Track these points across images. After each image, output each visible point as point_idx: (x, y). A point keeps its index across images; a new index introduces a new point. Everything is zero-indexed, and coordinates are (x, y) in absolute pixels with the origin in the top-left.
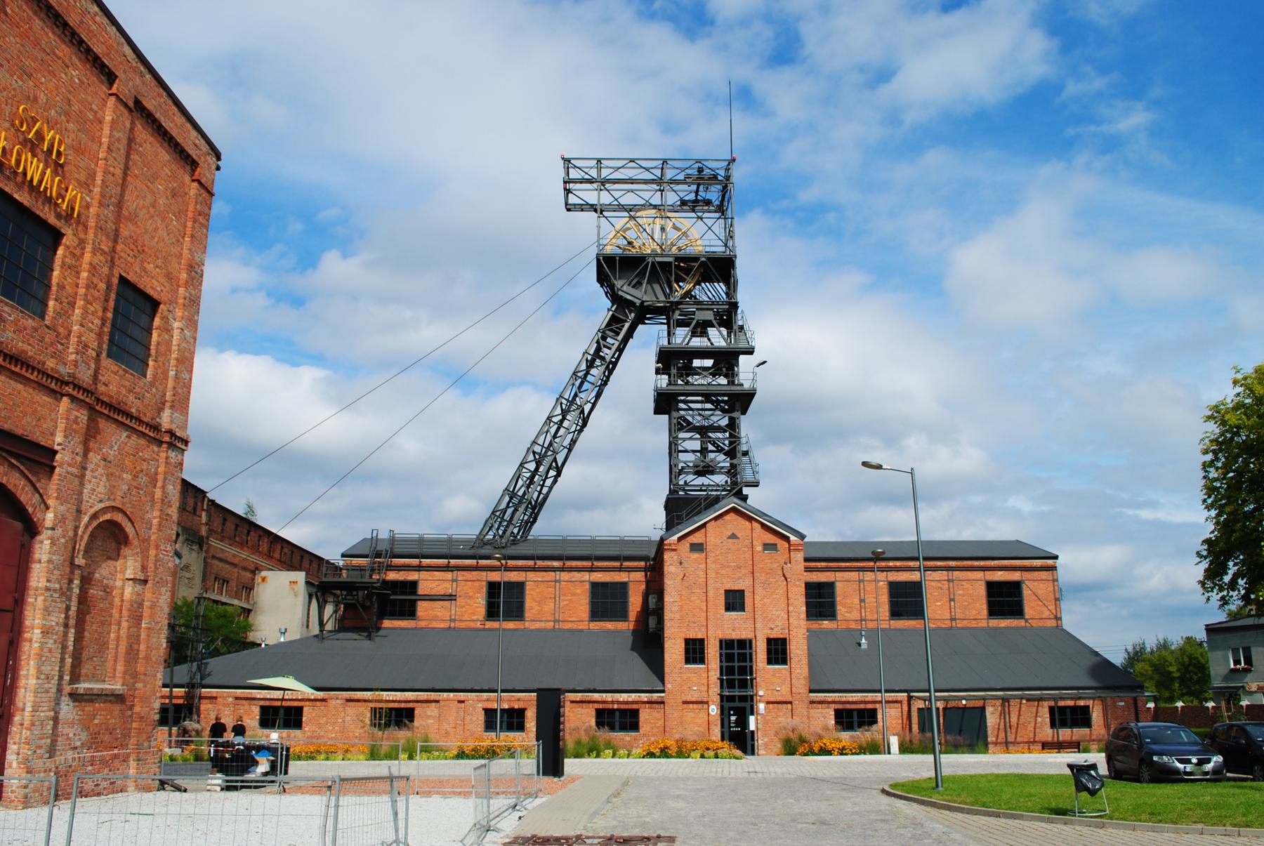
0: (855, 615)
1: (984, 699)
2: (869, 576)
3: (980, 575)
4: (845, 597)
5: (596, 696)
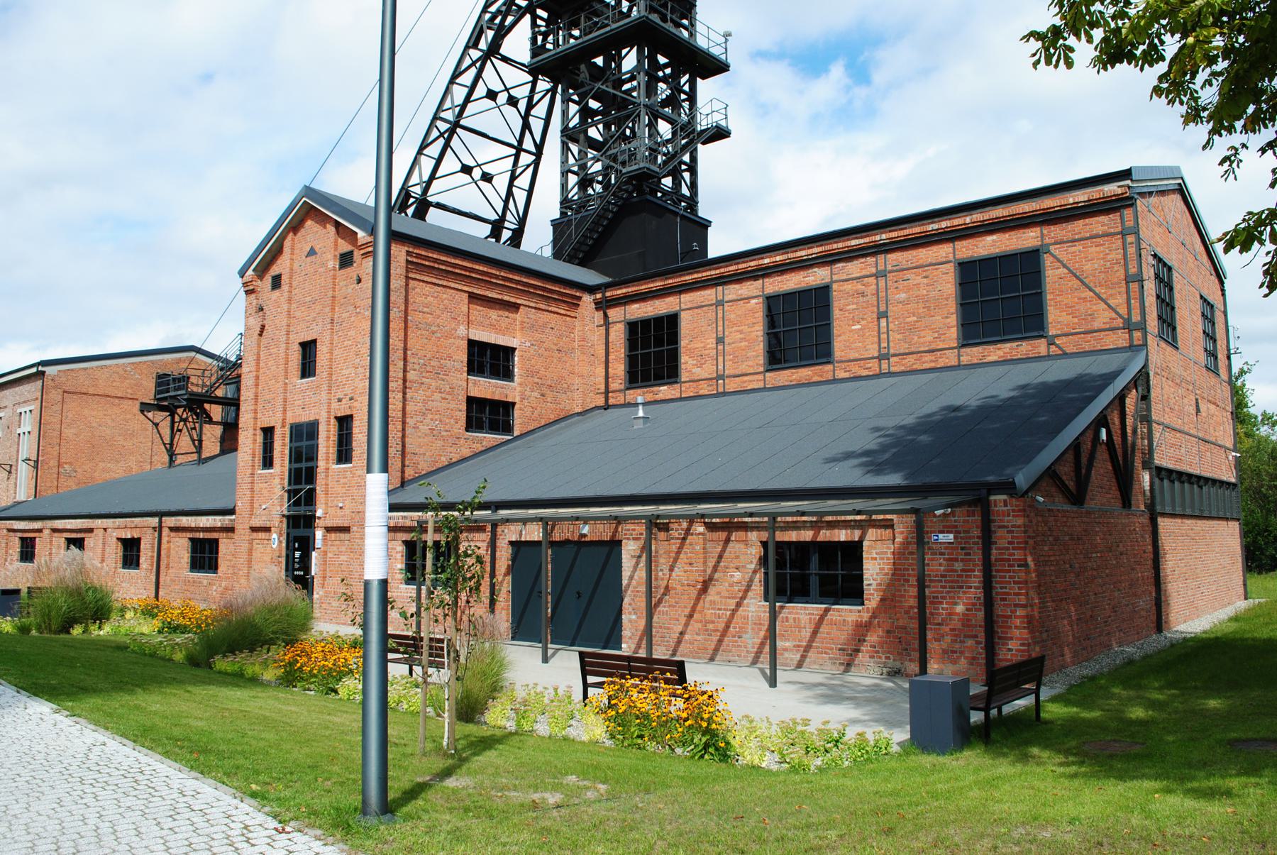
0: (708, 370)
1: (618, 520)
2: (733, 291)
4: (694, 338)
5: (185, 521)
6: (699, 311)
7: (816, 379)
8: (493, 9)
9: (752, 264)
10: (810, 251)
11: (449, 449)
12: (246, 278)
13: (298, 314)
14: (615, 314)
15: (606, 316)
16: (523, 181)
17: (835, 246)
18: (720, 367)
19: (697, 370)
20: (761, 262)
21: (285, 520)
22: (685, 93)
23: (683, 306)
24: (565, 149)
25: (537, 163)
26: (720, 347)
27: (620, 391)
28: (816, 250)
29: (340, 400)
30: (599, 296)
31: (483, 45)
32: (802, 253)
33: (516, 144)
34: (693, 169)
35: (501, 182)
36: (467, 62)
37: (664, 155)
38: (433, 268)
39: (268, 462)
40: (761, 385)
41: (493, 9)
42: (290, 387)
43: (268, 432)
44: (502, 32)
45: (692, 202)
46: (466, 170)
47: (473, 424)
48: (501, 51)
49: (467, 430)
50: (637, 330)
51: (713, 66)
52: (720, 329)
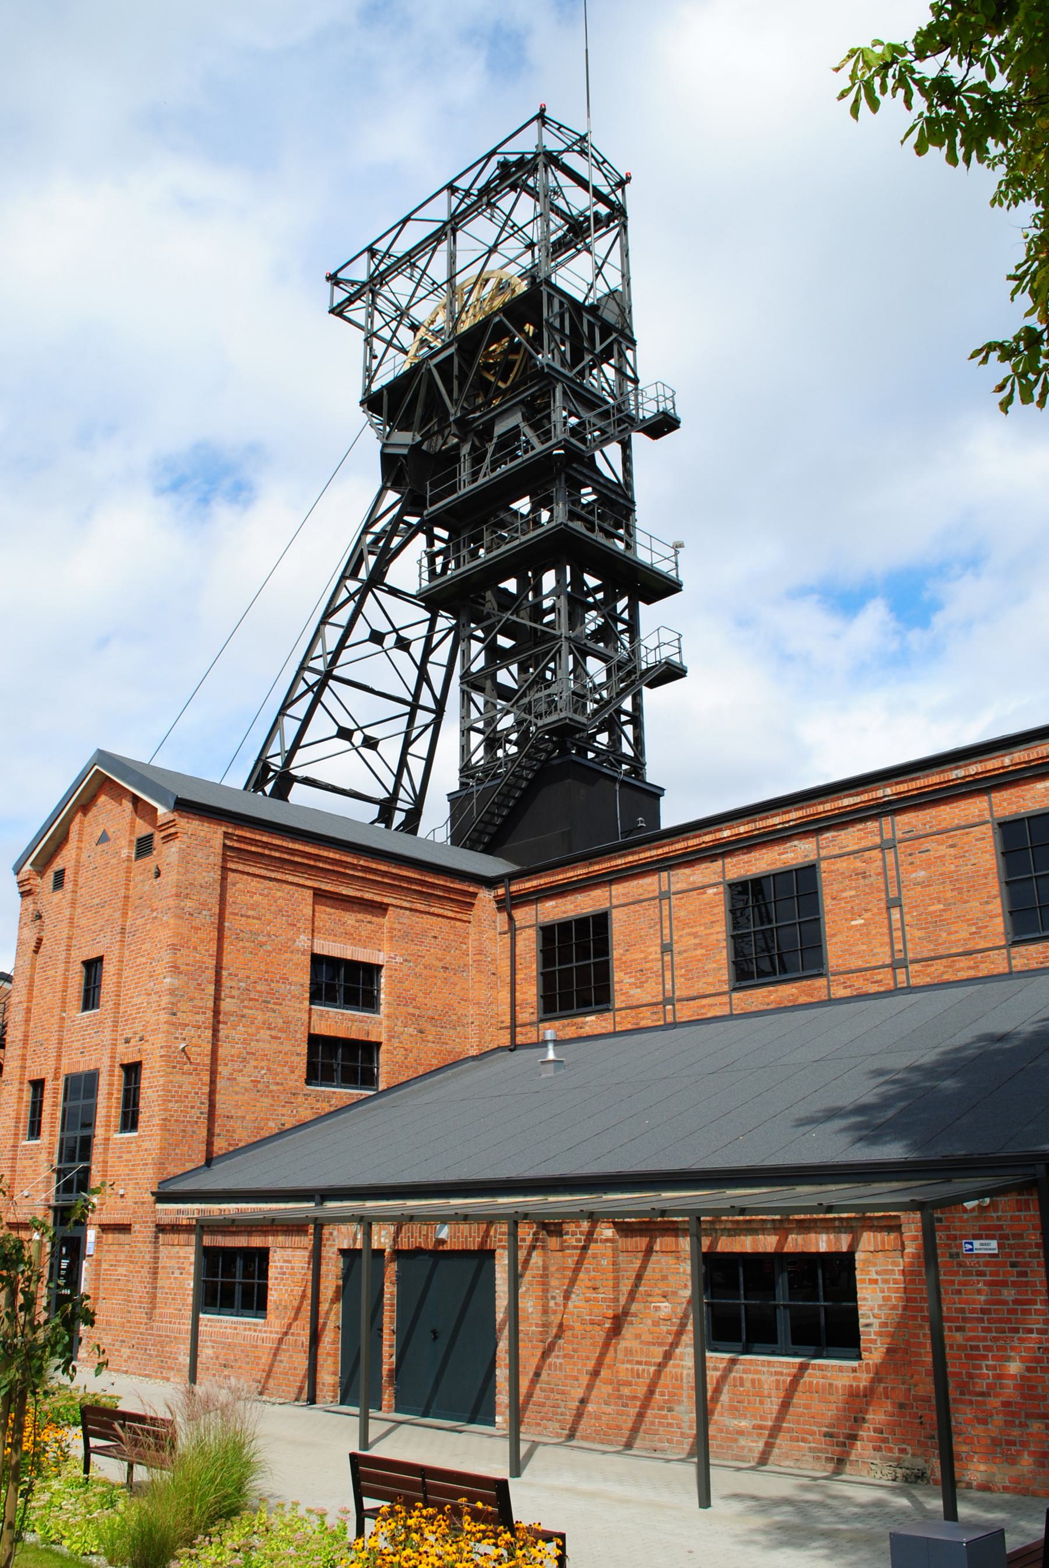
0: (650, 992)
1: (490, 1220)
3: (975, 807)
4: (629, 946)
6: (637, 907)
7: (803, 999)
8: (377, 528)
9: (707, 838)
10: (786, 817)
11: (281, 1110)
12: (23, 876)
13: (83, 922)
14: (524, 915)
15: (511, 918)
16: (421, 747)
17: (820, 808)
18: (668, 986)
19: (635, 992)
20: (719, 835)
21: (51, 1213)
22: (623, 621)
23: (615, 902)
24: (466, 700)
25: (437, 723)
26: (667, 958)
27: (531, 1024)
28: (794, 815)
29: (127, 1041)
30: (501, 891)
31: (363, 574)
32: (775, 820)
33: (410, 699)
34: (636, 719)
35: (391, 749)
36: (344, 595)
37: (596, 701)
38: (263, 855)
39: (35, 1131)
40: (726, 1011)
41: (377, 528)
42: (68, 1023)
43: (38, 1085)
44: (386, 558)
45: (638, 764)
46: (344, 734)
47: (316, 1074)
48: (387, 581)
49: (308, 1082)
50: (556, 939)
51: (661, 587)
52: (666, 931)
